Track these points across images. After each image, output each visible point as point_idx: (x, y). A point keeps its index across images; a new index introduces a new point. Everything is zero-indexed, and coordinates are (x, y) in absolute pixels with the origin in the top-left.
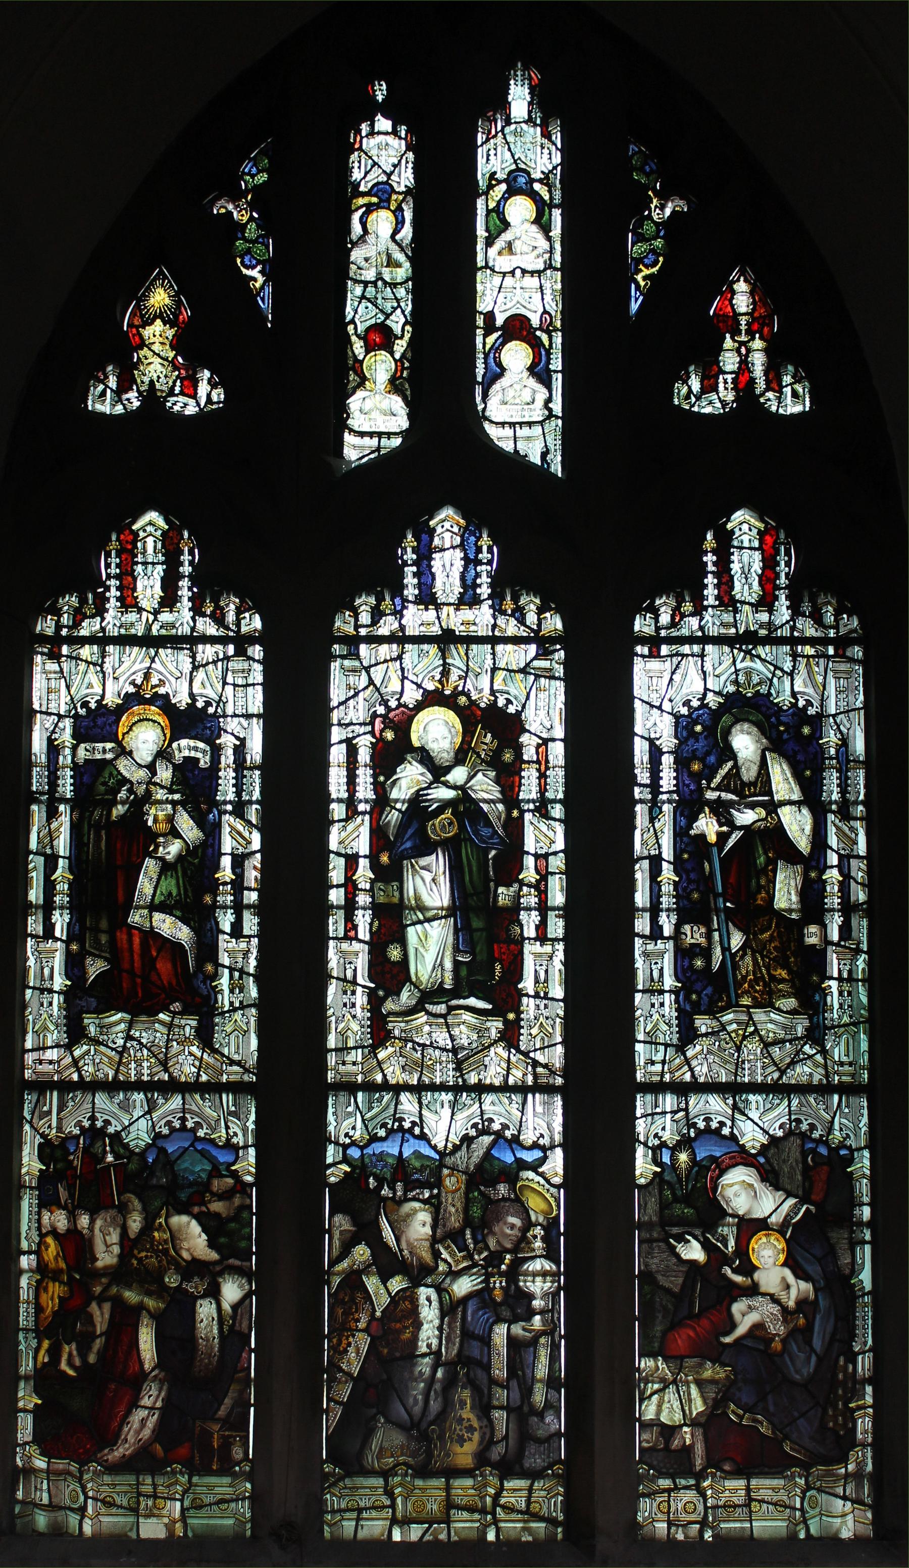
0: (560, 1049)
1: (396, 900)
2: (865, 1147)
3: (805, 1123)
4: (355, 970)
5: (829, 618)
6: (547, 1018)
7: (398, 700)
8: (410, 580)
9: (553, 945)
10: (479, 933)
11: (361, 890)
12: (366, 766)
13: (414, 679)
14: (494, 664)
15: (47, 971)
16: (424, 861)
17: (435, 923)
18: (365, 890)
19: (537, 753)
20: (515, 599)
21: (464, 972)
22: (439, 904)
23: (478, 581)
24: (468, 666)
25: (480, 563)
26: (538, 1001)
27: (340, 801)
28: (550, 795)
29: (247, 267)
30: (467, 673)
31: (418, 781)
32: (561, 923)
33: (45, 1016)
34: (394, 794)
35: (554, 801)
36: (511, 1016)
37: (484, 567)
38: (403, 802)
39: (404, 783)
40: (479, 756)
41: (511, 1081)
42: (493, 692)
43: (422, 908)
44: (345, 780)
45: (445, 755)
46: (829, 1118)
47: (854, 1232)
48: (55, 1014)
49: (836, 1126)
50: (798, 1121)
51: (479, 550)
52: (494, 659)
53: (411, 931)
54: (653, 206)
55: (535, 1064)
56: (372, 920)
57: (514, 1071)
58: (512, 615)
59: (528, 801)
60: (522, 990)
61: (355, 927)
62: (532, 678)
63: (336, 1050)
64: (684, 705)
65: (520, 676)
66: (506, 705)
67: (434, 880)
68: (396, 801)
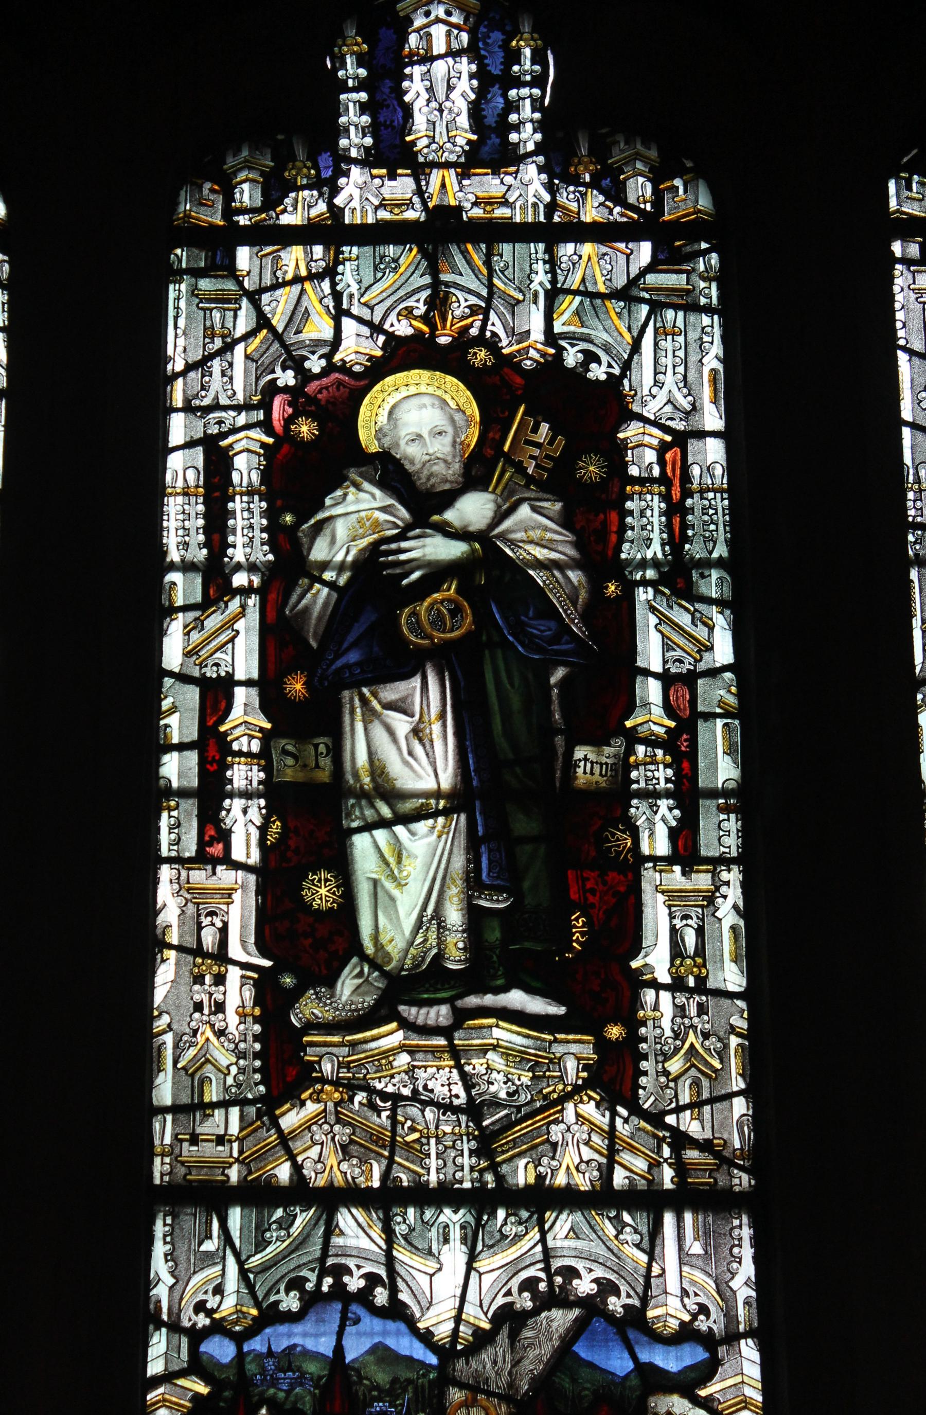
0: (740, 1106)
1: (324, 776)
4: (224, 930)
6: (706, 1036)
7: (329, 357)
9: (715, 874)
10: (528, 848)
11: (240, 754)
12: (250, 493)
13: (365, 314)
14: (554, 281)
16: (392, 692)
17: (422, 826)
18: (249, 755)
19: (661, 462)
21: (494, 935)
22: (429, 784)
23: (513, 118)
24: (490, 286)
25: (518, 83)
26: (681, 999)
27: (187, 567)
28: (695, 550)
30: (489, 300)
31: (377, 525)
32: (732, 824)
34: (319, 552)
35: (706, 564)
36: (615, 1032)
37: (525, 91)
38: (341, 568)
39: (341, 529)
40: (520, 469)
41: (620, 1178)
42: (551, 337)
43: (392, 795)
44: (201, 522)
45: (439, 468)
51: (515, 57)
52: (553, 272)
53: (361, 843)
55: (680, 1140)
56: (267, 821)
57: (626, 1157)
58: (593, 185)
59: (643, 564)
60: (639, 972)
61: (225, 836)
62: (645, 309)
63: (175, 1109)
65: (615, 306)
66: (585, 365)
67: (416, 732)
68: (325, 565)
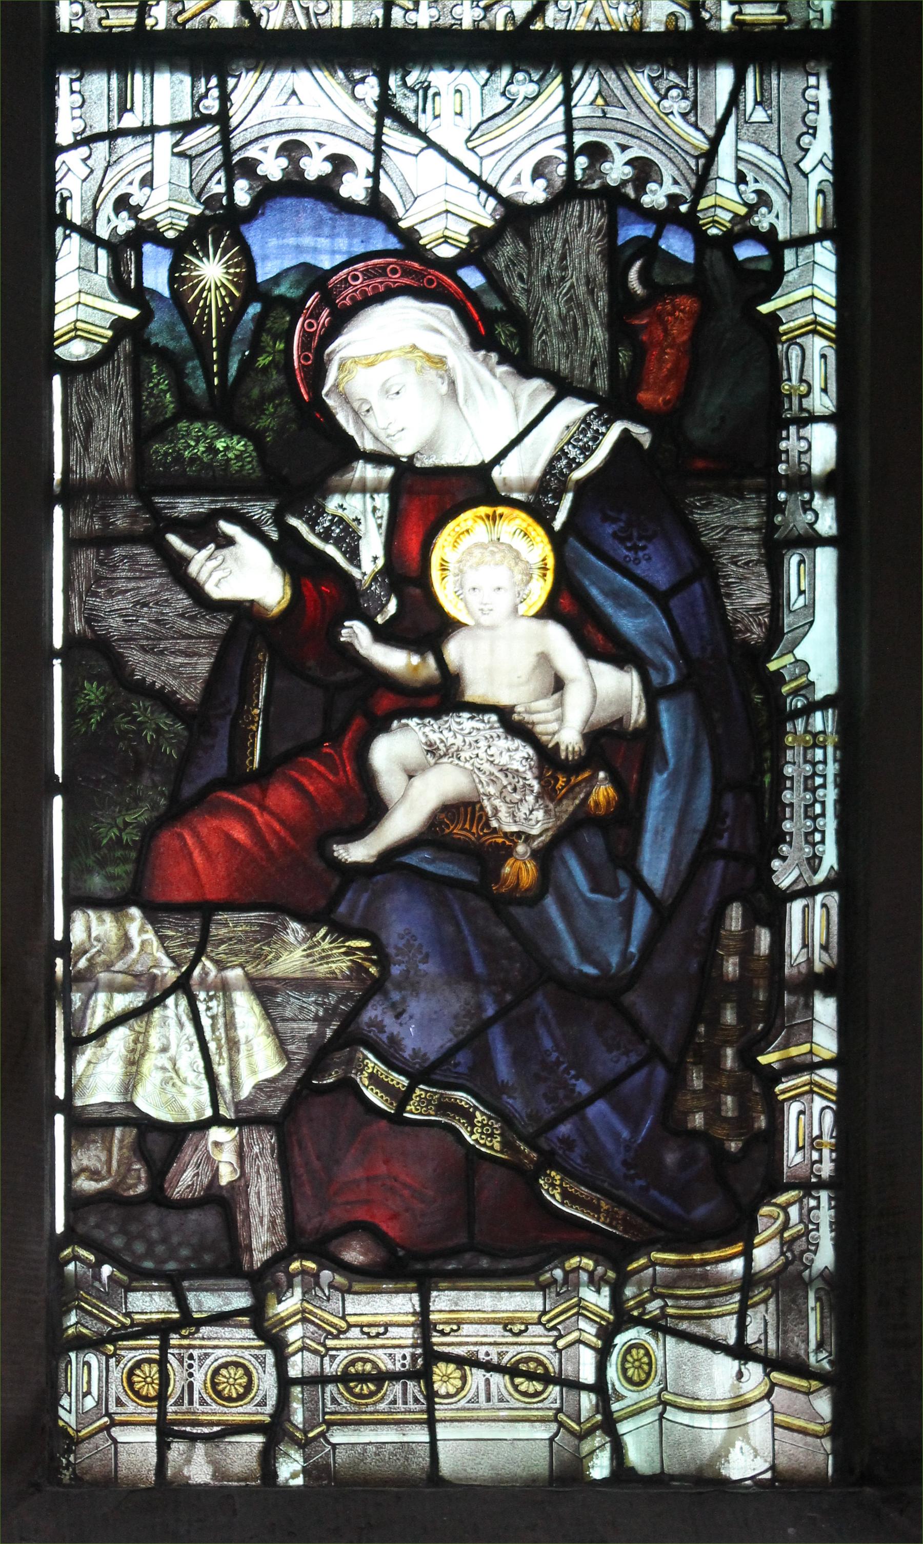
2: (821, 235)
3: (620, 158)
46: (705, 146)
47: (779, 508)
49: (725, 166)
50: (597, 152)
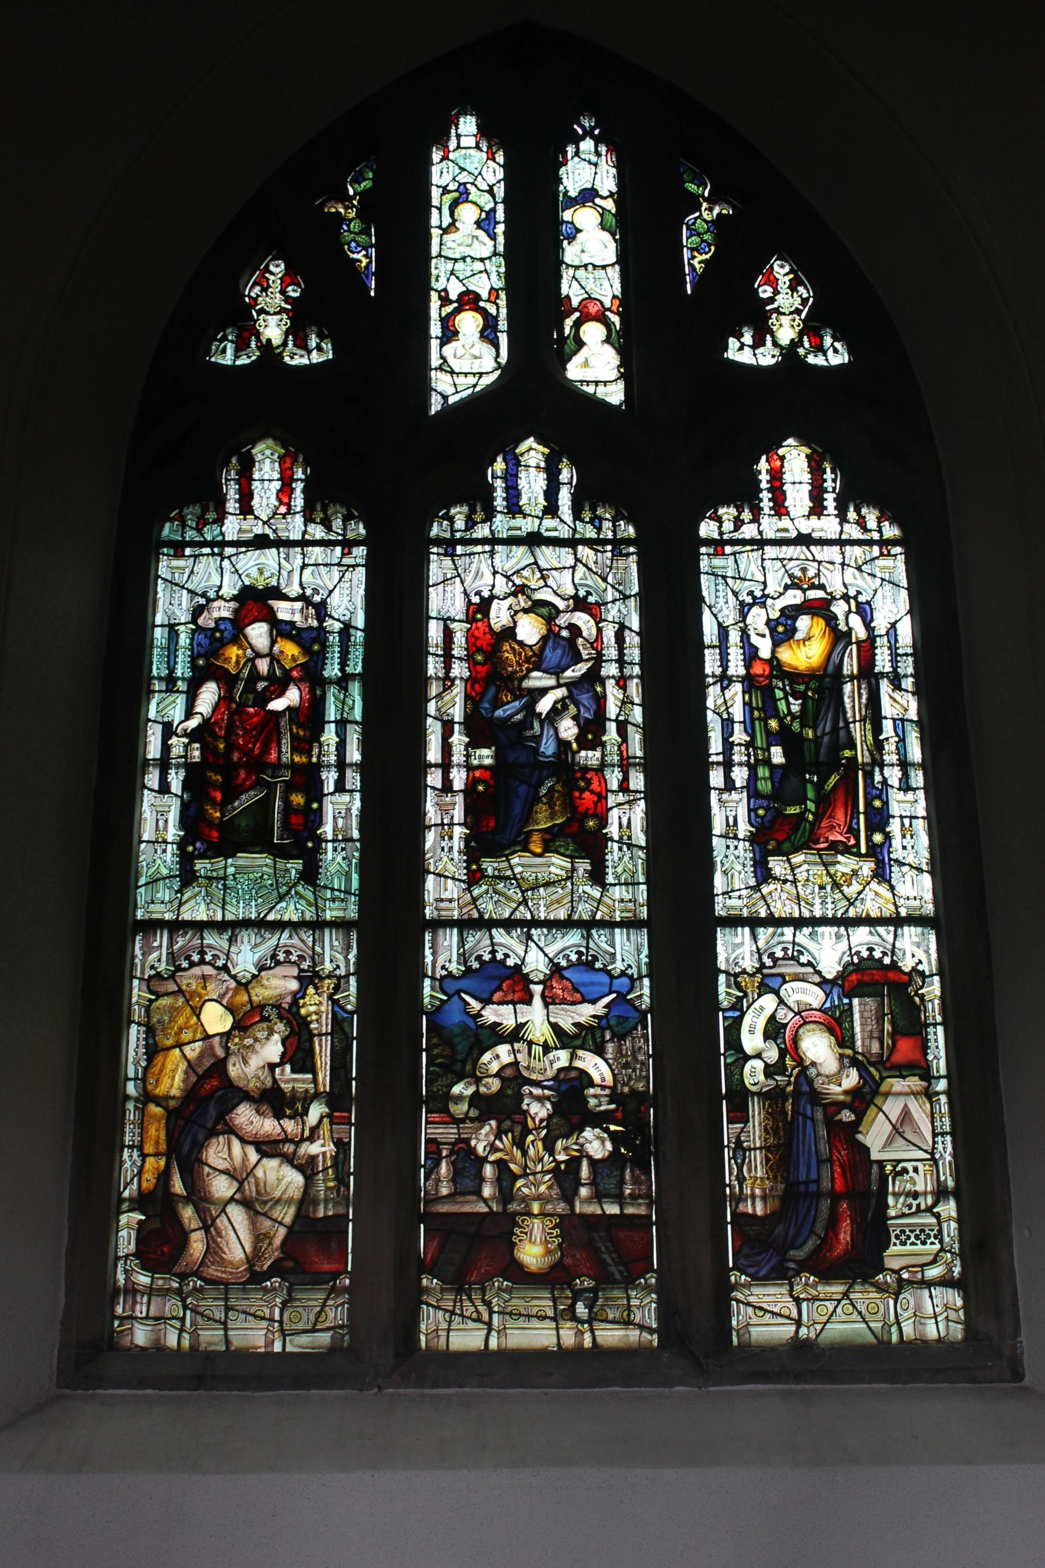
0: (643, 887)
5: (872, 524)
7: (491, 591)
8: (500, 494)
15: (161, 823)
20: (593, 510)
29: (353, 253)
32: (641, 776)
33: (159, 861)
48: (169, 861)
54: (703, 209)
64: (748, 594)
